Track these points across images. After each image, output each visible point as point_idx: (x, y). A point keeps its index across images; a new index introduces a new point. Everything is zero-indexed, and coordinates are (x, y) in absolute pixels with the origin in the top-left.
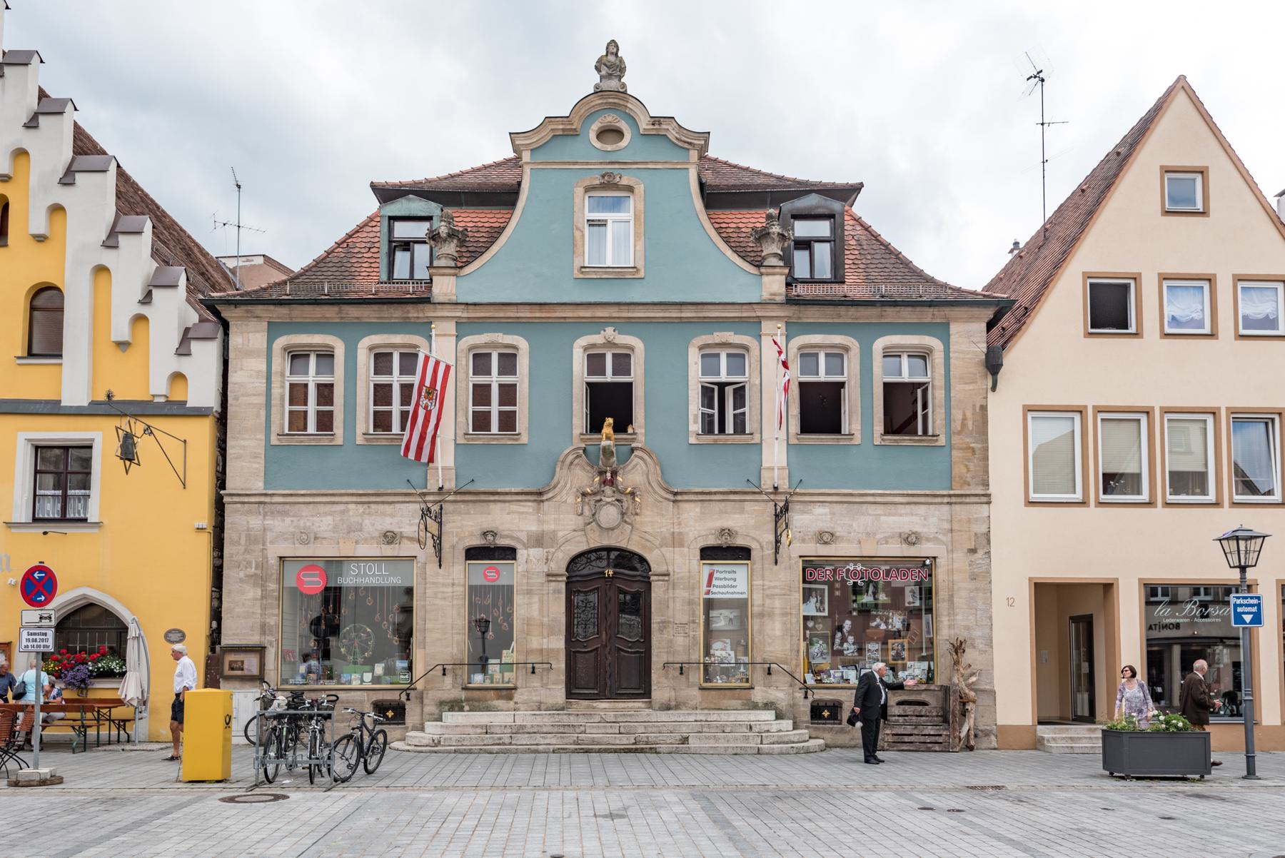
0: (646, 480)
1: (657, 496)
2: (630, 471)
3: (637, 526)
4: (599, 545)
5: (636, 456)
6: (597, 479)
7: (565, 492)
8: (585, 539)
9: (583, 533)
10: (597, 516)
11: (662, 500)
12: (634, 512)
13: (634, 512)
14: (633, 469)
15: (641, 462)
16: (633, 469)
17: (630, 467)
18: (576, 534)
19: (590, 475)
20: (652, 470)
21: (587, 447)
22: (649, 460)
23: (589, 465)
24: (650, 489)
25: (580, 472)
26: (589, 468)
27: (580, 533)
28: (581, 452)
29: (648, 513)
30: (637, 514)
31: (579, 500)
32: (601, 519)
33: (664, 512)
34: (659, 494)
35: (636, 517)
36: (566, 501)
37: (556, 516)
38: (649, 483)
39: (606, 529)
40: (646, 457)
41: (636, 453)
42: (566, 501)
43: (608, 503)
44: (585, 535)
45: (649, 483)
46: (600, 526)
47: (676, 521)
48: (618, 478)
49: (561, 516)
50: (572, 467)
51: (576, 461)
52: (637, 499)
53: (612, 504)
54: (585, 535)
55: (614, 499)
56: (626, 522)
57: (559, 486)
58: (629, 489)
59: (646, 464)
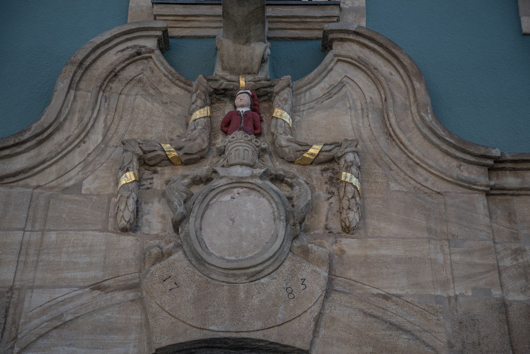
1: (421, 175)
5: (341, 59)
6: (200, 114)
7: (77, 157)
10: (191, 225)
11: (443, 187)
13: (336, 226)
15: (360, 78)
17: (318, 91)
18: (103, 299)
20: (400, 98)
22: (385, 68)
24: (396, 153)
25: (140, 100)
26: (175, 90)
27: (119, 296)
28: (151, 44)
29: (393, 229)
30: (347, 230)
31: (129, 177)
32: (207, 235)
36: (78, 186)
38: (391, 136)
40: (374, 60)
41: (338, 48)
43: (239, 182)
44: (140, 300)
45: (391, 136)
46: (201, 261)
47: (507, 262)
48: (278, 112)
49: (53, 236)
50: (115, 85)
51: (132, 71)
52: (346, 176)
54: (140, 300)
55: (259, 171)
56: (306, 252)
57: (59, 138)
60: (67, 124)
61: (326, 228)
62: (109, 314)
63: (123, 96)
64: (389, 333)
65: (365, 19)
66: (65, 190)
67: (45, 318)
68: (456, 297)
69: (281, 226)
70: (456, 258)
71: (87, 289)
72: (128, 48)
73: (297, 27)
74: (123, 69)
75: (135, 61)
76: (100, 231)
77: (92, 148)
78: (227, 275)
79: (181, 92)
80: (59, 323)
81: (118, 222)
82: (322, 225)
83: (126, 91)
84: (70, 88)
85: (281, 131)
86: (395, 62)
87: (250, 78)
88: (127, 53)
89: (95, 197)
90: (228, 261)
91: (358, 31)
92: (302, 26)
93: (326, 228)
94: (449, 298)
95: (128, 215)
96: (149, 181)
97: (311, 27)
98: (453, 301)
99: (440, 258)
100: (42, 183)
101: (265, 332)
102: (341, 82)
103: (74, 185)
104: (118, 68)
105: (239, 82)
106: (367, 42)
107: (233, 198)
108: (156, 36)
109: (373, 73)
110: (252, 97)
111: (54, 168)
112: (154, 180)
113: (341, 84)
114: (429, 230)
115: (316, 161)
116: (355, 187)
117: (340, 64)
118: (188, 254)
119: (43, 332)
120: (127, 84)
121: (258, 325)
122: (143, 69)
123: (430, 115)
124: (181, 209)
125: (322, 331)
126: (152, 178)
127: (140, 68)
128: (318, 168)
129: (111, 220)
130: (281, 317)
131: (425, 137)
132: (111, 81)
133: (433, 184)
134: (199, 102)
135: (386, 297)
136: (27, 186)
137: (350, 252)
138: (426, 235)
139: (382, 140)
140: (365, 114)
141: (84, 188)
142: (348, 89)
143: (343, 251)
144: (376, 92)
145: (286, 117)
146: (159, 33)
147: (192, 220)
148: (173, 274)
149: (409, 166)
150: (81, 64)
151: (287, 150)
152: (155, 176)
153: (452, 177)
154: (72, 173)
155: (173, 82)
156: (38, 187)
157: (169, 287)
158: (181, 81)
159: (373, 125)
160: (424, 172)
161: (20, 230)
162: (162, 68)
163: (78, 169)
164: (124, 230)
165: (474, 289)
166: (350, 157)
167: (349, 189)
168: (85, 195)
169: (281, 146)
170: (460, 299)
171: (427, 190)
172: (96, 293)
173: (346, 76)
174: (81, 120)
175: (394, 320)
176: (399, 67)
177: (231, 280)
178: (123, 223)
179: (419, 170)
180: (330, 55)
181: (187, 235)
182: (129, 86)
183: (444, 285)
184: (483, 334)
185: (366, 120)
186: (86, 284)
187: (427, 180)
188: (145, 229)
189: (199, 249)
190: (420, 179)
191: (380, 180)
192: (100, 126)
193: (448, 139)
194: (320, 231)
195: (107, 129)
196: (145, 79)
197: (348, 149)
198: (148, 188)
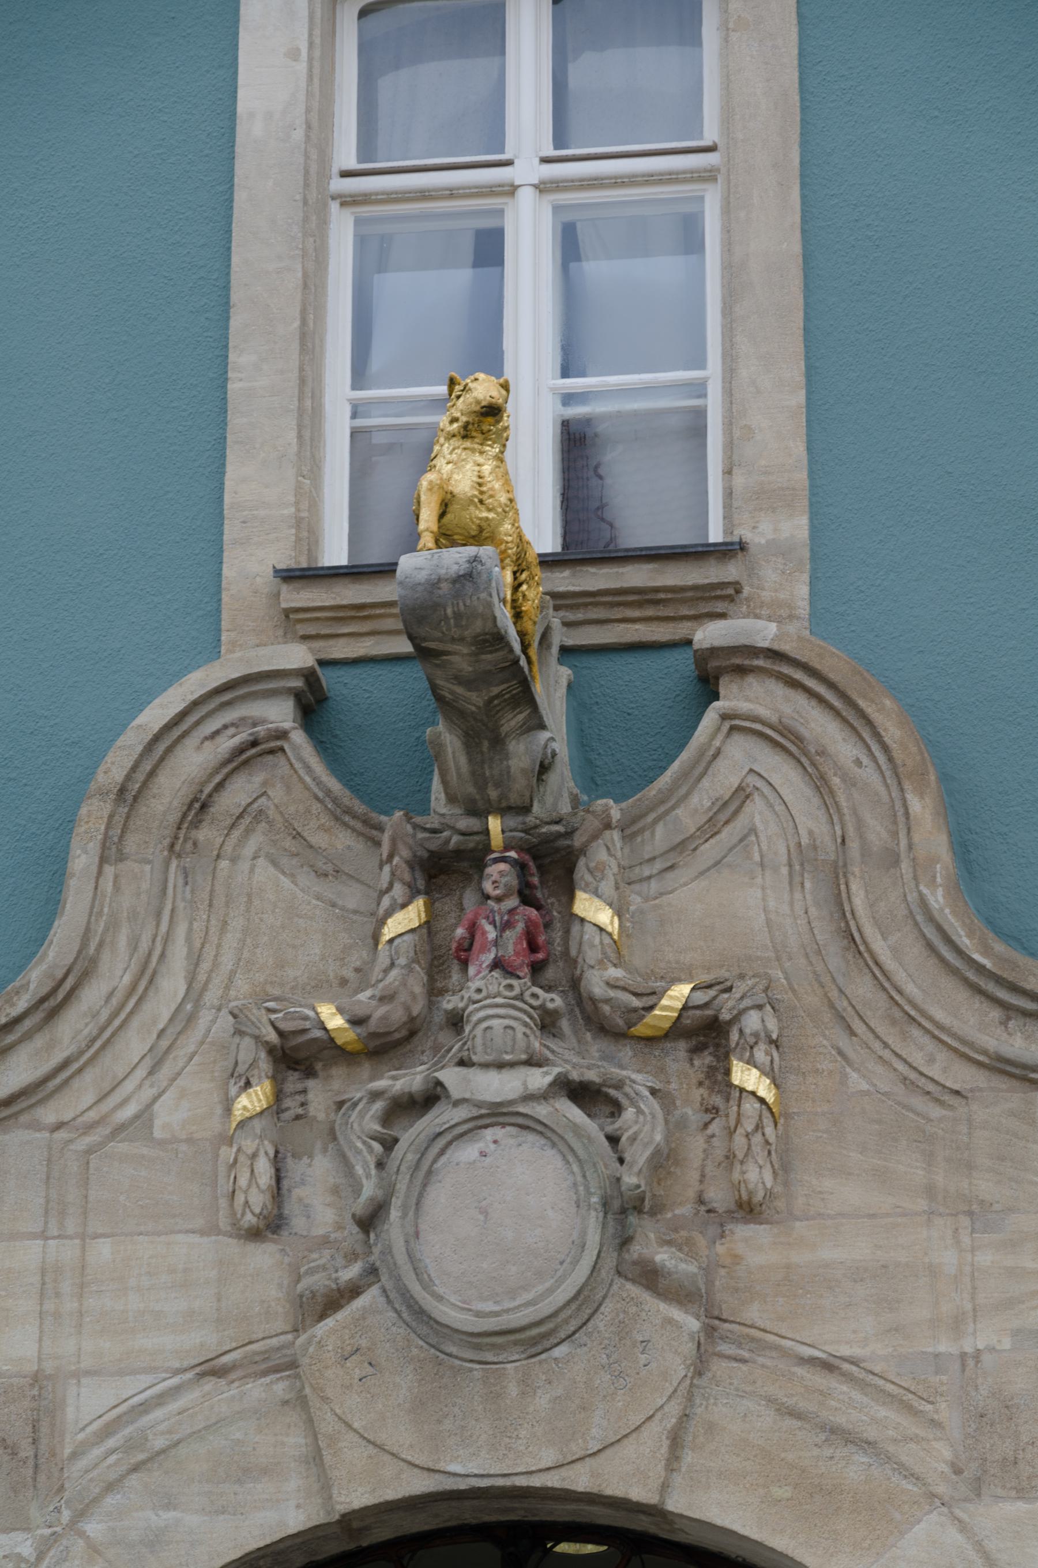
0: (824, 931)
2: (683, 847)
3: (753, 1313)
4: (419, 1485)
8: (296, 1441)
9: (280, 1387)
12: (719, 1196)
13: (719, 1196)
14: (711, 828)
16: (711, 828)
19: (353, 897)
20: (877, 831)
21: (326, 677)
23: (341, 815)
24: (862, 988)
25: (265, 870)
27: (256, 1390)
33: (985, 1187)
34: (938, 1032)
35: (742, 1231)
36: (145, 1116)
37: (67, 1252)
39: (477, 1340)
42: (145, 1116)
49: (103, 1251)
50: (204, 834)
53: (529, 1125)
54: (302, 1401)
55: (539, 1079)
57: (92, 995)
58: (680, 992)
59: (820, 784)
60: (106, 956)
61: (701, 1201)
62: (238, 1435)
63: (224, 864)
64: (828, 1452)
65: (806, 577)
66: (120, 1128)
67: (111, 1443)
68: (977, 1355)
69: (593, 1220)
70: (985, 1258)
71: (189, 1375)
72: (225, 727)
73: (636, 613)
74: (220, 786)
75: (246, 762)
76: (202, 1233)
77: (166, 1015)
78: (478, 1347)
79: (359, 846)
80: (141, 1457)
81: (239, 1216)
82: (691, 1194)
83: (228, 848)
84: (103, 860)
85: (591, 955)
86: (866, 735)
87: (513, 821)
88: (227, 744)
89: (183, 1147)
90: (478, 1314)
91: (776, 647)
92: (650, 612)
93: (701, 1201)
94: (963, 1355)
95: (258, 1200)
96: (300, 1098)
97: (669, 612)
98: (971, 1363)
99: (948, 1259)
100: (67, 1116)
101: (564, 1472)
102: (740, 788)
103: (137, 1117)
104: (208, 790)
105: (487, 832)
106: (798, 675)
107: (483, 1154)
108: (290, 691)
109: (813, 764)
110: (521, 867)
111: (88, 1076)
112: (311, 1096)
113: (742, 795)
114: (930, 1191)
115: (677, 1031)
116: (762, 1101)
117: (738, 738)
118: (393, 1295)
119: (112, 1476)
120: (233, 826)
121: (548, 1457)
122: (265, 783)
123: (940, 892)
124: (369, 1189)
125: (689, 1457)
126: (304, 1091)
127: (258, 778)
128: (682, 1045)
129: (223, 1203)
130: (596, 1435)
131: (930, 946)
132: (196, 824)
133: (945, 1070)
134: (399, 891)
135: (827, 1366)
136: (36, 1126)
137: (755, 1259)
138: (922, 1204)
139: (835, 957)
140: (797, 879)
141: (158, 1123)
142: (756, 812)
143: (737, 1259)
144: (821, 814)
145: (604, 917)
146: (298, 683)
147: (394, 1214)
148: (364, 1343)
149: (894, 1022)
150: (122, 790)
151: (606, 1009)
152: (311, 1083)
153: (985, 1052)
154: (129, 1086)
155: (337, 819)
156: (59, 1126)
157: (357, 1373)
158: (355, 816)
159: (813, 911)
160: (926, 1040)
161: (33, 1236)
162: (308, 779)
163: (141, 1073)
164: (255, 1235)
165: (1016, 1333)
166: (752, 1021)
167: (750, 1107)
168: (161, 1143)
169: (593, 1000)
170: (987, 1358)
171: (931, 1087)
172: (209, 1384)
173: (751, 770)
174: (134, 945)
175: (841, 1420)
176: (875, 748)
177: (489, 1357)
178: (249, 1219)
179: (916, 1032)
180: (710, 717)
181: (388, 1251)
182: (236, 834)
183: (957, 1324)
184: (1025, 1438)
185: (798, 896)
186: (186, 1364)
187: (931, 1060)
188: (298, 1223)
189: (416, 1289)
190: (918, 1059)
191: (825, 1065)
192: (179, 952)
193: (976, 957)
194: (685, 1210)
195: (195, 961)
196: (272, 813)
197: (747, 1002)
198: (298, 1117)
